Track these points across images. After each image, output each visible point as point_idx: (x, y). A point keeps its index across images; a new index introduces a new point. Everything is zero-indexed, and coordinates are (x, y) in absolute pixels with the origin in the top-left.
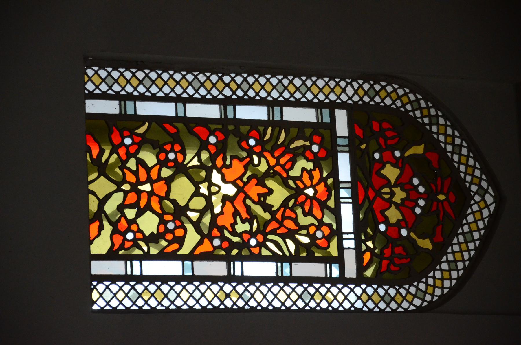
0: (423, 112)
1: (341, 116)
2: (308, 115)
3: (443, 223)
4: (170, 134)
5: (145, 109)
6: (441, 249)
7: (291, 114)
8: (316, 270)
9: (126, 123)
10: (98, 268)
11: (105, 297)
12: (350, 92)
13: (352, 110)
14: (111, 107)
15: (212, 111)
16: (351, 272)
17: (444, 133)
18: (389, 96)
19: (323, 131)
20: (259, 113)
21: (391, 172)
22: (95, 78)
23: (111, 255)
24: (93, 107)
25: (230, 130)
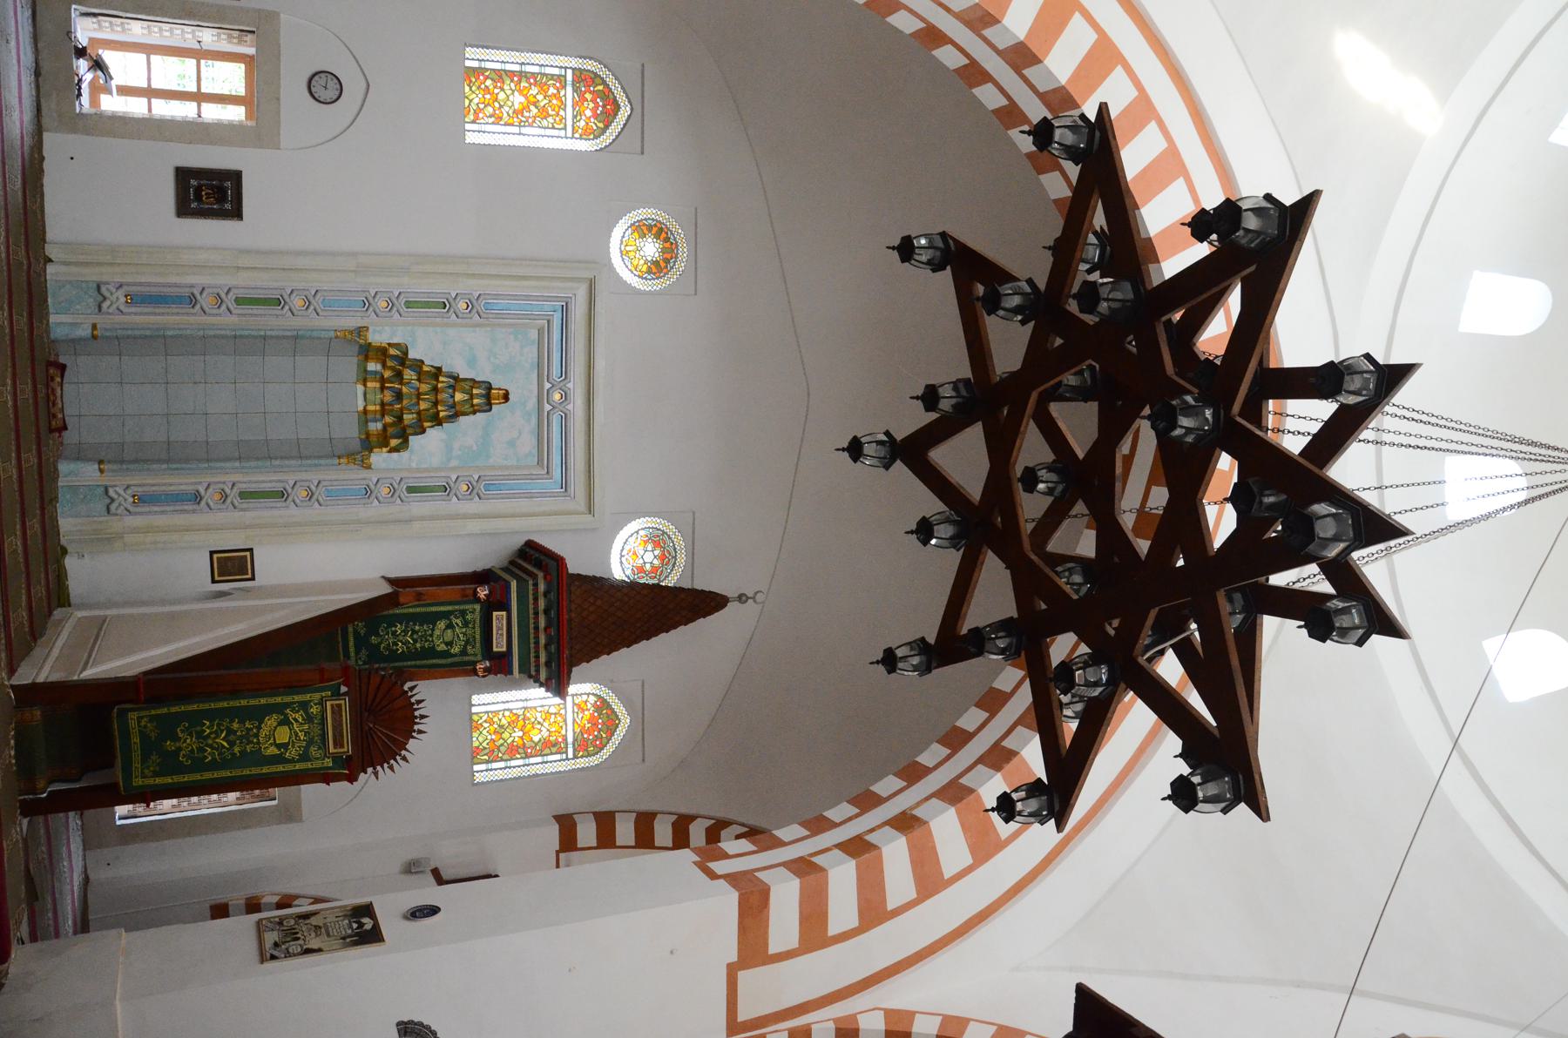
0: (604, 72)
1: (569, 72)
2: (556, 71)
3: (608, 116)
4: (500, 76)
5: (489, 65)
6: (607, 126)
7: (548, 70)
8: (555, 132)
9: (478, 72)
10: (468, 126)
11: (471, 138)
12: (575, 62)
13: (574, 69)
14: (475, 64)
15: (516, 68)
16: (569, 134)
17: (611, 80)
18: (590, 65)
19: (561, 79)
20: (535, 69)
21: (588, 96)
22: (470, 52)
23: (473, 122)
24: (468, 63)
25: (522, 75)
